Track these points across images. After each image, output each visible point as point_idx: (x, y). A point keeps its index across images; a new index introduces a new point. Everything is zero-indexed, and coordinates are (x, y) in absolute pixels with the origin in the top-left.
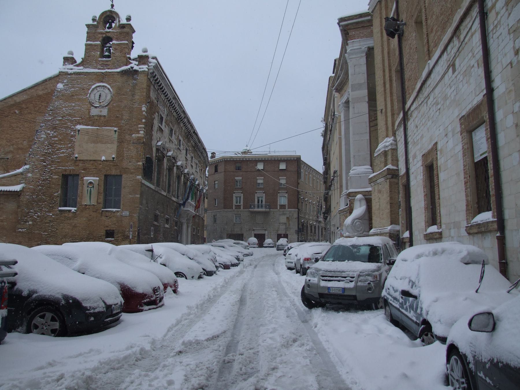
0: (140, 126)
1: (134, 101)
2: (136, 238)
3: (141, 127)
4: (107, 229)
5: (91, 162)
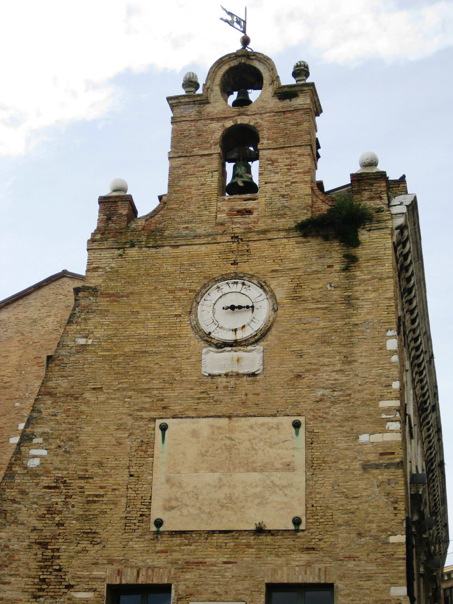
1: (354, 320)
3: (388, 410)
5: (216, 539)
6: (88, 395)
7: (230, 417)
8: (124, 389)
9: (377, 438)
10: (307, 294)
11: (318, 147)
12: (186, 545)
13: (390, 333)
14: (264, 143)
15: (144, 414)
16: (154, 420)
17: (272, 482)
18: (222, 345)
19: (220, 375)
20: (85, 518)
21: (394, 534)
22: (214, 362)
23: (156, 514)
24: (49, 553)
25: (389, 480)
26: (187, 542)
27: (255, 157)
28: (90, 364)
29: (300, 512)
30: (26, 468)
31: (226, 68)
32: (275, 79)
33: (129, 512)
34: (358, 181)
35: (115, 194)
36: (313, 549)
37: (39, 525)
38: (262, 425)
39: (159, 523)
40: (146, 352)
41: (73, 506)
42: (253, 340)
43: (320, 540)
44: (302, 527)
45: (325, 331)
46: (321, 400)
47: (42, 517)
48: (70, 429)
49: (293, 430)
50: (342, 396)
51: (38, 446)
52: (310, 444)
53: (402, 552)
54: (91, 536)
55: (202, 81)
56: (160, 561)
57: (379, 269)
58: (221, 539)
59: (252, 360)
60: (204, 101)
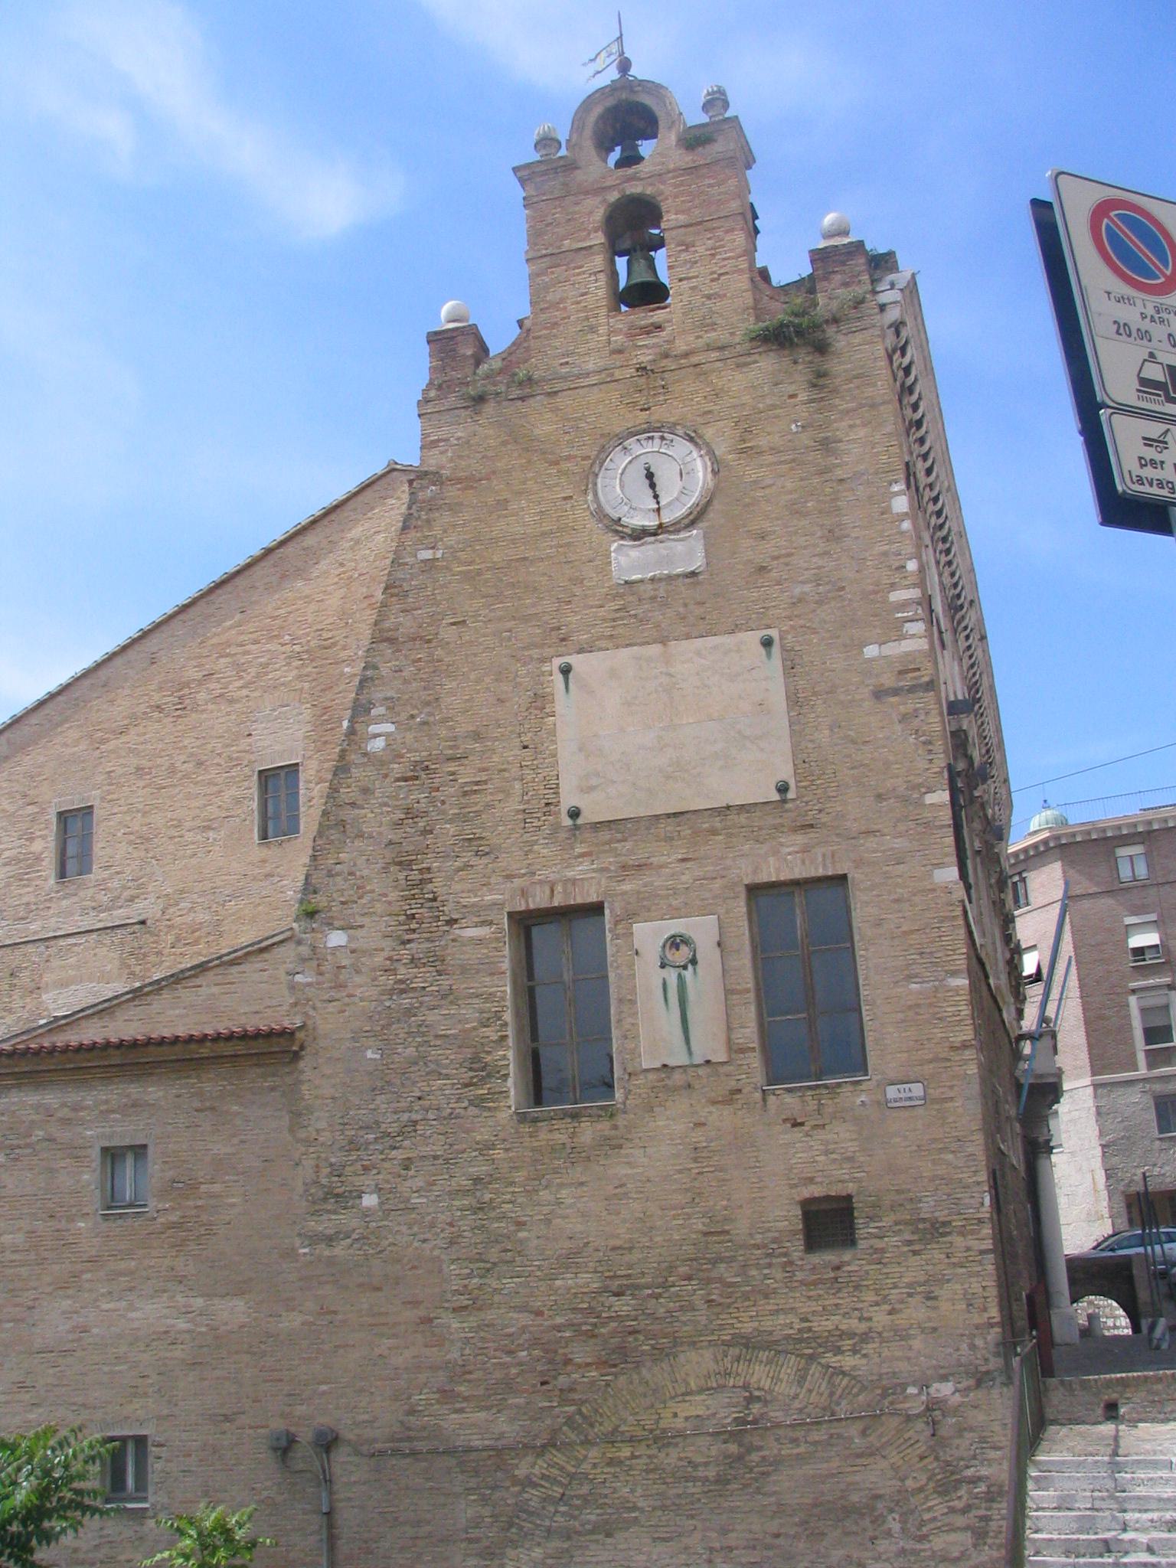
0: (896, 596)
1: (839, 473)
2: (987, 1231)
3: (903, 605)
4: (808, 1192)
6: (448, 634)
7: (663, 641)
8: (500, 619)
9: (894, 649)
10: (763, 442)
11: (755, 217)
12: (619, 841)
13: (896, 488)
14: (670, 219)
15: (535, 653)
16: (549, 659)
17: (739, 732)
18: (640, 535)
19: (642, 581)
20: (462, 818)
21: (930, 791)
22: (629, 562)
23: (568, 800)
24: (415, 876)
25: (916, 710)
26: (619, 836)
27: (660, 244)
28: (442, 587)
29: (786, 773)
30: (365, 754)
31: (598, 110)
32: (676, 118)
33: (528, 802)
34: (822, 260)
35: (451, 326)
36: (812, 826)
37: (396, 838)
38: (715, 647)
39: (574, 814)
40: (525, 559)
41: (443, 802)
42: (686, 521)
43: (820, 811)
44: (791, 795)
45: (795, 496)
46: (800, 600)
47: (398, 824)
48: (425, 689)
49: (762, 651)
50: (829, 591)
51: (380, 720)
52: (790, 668)
53: (946, 816)
54: (476, 845)
55: (563, 136)
56: (580, 870)
57: (869, 392)
58: (669, 827)
59: (687, 553)
60: (569, 166)
